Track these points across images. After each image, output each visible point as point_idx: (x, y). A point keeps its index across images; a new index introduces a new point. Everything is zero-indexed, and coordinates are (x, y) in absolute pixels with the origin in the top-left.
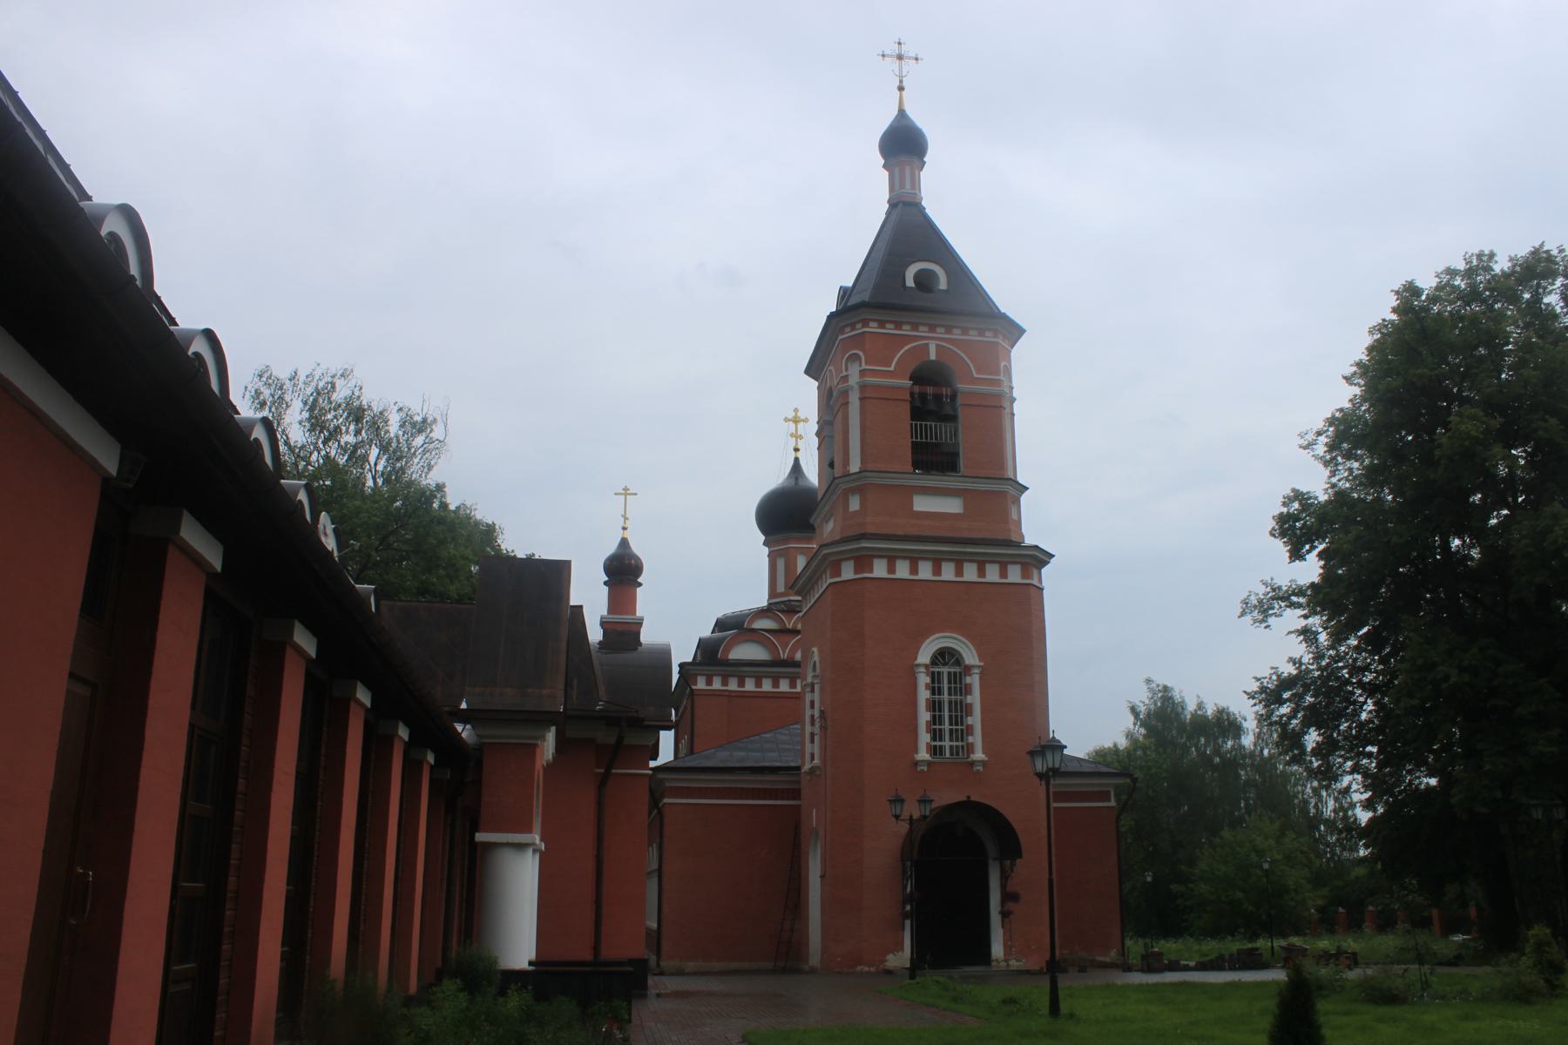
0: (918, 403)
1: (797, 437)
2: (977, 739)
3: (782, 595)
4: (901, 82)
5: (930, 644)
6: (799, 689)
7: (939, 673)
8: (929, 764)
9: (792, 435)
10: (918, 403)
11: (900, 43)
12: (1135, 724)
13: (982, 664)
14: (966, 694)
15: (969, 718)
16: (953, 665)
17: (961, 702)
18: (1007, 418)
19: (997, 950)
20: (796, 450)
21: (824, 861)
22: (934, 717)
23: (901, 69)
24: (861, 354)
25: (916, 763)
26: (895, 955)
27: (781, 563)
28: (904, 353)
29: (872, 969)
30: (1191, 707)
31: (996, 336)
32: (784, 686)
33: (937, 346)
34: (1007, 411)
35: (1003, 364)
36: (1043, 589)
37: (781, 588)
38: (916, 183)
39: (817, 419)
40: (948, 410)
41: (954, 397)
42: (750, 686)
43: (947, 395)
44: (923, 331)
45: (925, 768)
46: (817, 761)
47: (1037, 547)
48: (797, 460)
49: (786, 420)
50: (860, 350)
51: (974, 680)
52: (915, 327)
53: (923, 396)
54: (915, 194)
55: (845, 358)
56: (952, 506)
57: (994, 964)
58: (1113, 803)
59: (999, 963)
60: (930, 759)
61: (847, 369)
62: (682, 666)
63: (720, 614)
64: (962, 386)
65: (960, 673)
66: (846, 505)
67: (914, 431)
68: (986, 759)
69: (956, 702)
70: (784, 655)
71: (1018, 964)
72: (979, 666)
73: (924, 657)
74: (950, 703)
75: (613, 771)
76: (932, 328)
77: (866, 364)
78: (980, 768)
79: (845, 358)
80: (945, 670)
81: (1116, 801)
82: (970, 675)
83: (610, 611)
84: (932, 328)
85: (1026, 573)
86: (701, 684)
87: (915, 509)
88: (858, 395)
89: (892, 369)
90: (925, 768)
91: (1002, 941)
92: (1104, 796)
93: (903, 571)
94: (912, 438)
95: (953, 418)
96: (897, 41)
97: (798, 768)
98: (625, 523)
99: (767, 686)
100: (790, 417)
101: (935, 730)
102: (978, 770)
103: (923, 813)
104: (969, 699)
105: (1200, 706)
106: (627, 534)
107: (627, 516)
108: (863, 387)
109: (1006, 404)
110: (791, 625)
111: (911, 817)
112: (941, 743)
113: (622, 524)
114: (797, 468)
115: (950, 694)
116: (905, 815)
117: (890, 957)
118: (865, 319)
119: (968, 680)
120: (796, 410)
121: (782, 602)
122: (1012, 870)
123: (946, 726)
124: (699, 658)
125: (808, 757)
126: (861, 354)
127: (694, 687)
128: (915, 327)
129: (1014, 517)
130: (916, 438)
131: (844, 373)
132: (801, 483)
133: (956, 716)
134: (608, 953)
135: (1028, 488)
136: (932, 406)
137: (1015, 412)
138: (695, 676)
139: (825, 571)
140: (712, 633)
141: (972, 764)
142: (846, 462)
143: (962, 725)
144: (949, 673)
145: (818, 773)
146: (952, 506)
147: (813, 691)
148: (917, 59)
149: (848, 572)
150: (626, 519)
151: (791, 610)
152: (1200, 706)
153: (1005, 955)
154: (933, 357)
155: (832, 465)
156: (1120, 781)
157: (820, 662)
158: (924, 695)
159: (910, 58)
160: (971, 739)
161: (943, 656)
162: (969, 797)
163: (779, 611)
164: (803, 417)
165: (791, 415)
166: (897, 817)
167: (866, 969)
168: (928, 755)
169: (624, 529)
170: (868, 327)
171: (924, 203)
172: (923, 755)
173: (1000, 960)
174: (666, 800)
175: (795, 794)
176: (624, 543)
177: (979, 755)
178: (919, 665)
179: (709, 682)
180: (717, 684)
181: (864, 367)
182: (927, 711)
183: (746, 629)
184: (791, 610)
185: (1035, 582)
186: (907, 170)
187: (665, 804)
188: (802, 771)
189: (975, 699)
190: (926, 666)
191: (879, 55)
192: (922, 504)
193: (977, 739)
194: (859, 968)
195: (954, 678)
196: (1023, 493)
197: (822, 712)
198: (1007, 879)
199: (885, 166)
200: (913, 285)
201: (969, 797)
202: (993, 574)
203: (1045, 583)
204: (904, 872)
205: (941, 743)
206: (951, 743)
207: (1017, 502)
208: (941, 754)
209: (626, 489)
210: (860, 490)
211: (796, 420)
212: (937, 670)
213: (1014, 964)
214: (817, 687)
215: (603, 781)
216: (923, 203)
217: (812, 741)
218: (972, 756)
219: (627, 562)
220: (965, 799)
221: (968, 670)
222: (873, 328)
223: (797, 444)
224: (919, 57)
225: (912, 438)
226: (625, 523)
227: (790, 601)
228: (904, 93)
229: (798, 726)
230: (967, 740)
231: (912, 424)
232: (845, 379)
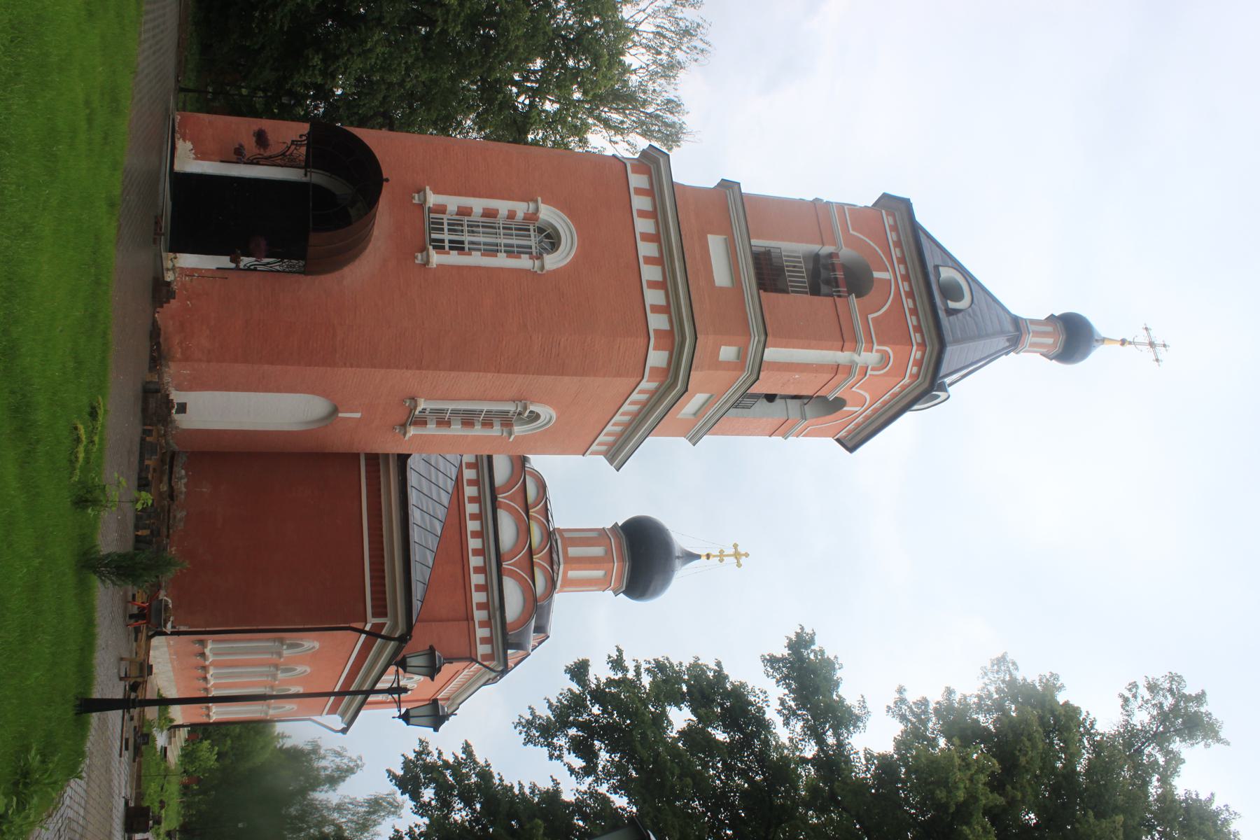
1: (721, 556)
2: (454, 258)
8: (422, 205)
9: (721, 552)
19: (188, 261)
25: (421, 190)
33: (890, 281)
37: (566, 535)
40: (824, 289)
43: (839, 291)
44: (900, 269)
45: (416, 201)
48: (698, 557)
49: (735, 546)
51: (524, 262)
53: (833, 268)
56: (721, 276)
57: (171, 255)
59: (171, 260)
70: (501, 498)
72: (542, 267)
73: (547, 213)
76: (906, 278)
89: (851, 232)
90: (416, 201)
91: (200, 266)
112: (446, 230)
117: (189, 145)
120: (747, 555)
128: (902, 260)
132: (677, 562)
136: (824, 274)
141: (423, 249)
146: (721, 276)
153: (182, 269)
154: (876, 275)
161: (551, 239)
162: (387, 180)
165: (741, 550)
172: (433, 199)
177: (436, 258)
192: (716, 244)
201: (387, 180)
205: (446, 230)
211: (737, 555)
212: (532, 233)
220: (384, 177)
228: (1118, 345)
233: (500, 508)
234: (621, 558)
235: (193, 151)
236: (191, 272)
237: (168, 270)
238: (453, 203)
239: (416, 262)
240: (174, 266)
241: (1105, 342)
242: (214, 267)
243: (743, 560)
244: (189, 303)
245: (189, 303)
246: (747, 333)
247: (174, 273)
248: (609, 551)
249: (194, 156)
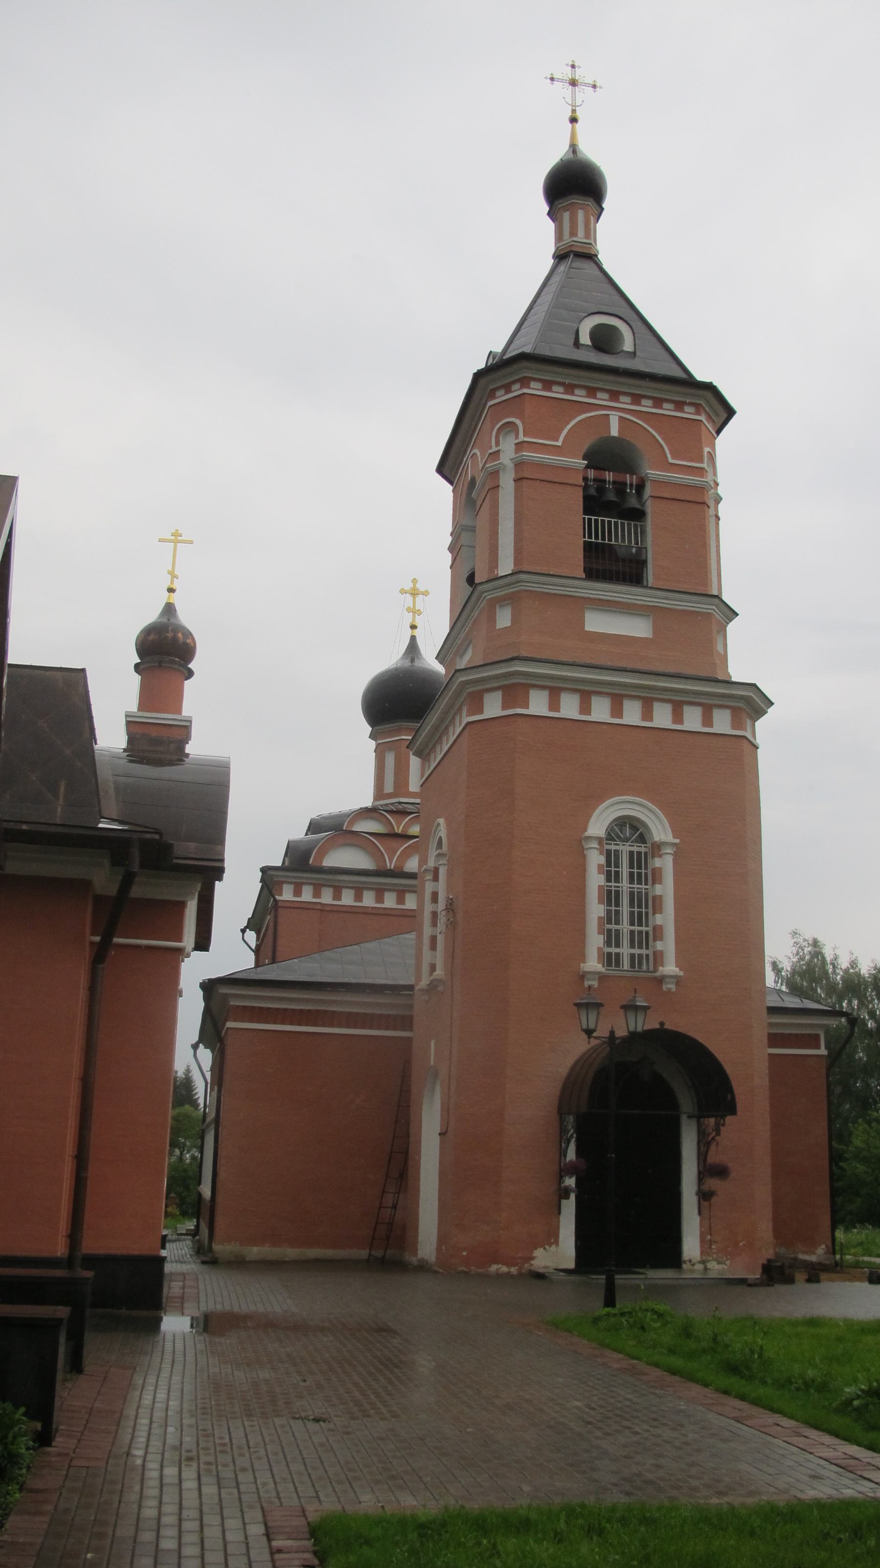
0: (592, 492)
1: (415, 612)
2: (668, 946)
3: (390, 796)
4: (574, 111)
5: (607, 808)
6: (411, 903)
7: (616, 851)
8: (602, 978)
9: (409, 610)
10: (592, 492)
11: (573, 66)
12: (776, 982)
13: (677, 841)
14: (654, 883)
15: (658, 916)
16: (636, 841)
17: (646, 894)
18: (712, 520)
20: (413, 627)
21: (446, 1110)
22: (609, 912)
23: (574, 98)
24: (518, 422)
25: (583, 976)
26: (544, 1249)
27: (390, 759)
28: (573, 426)
29: (514, 1270)
30: (844, 963)
31: (698, 413)
32: (390, 901)
33: (620, 418)
34: (711, 511)
35: (707, 450)
36: (757, 748)
37: (389, 788)
38: (590, 232)
39: (450, 530)
40: (633, 503)
41: (640, 487)
42: (347, 899)
43: (631, 485)
44: (602, 399)
46: (439, 973)
47: (754, 685)
48: (413, 638)
49: (403, 592)
50: (517, 418)
51: (666, 864)
52: (592, 392)
53: (600, 482)
54: (590, 244)
55: (496, 429)
57: (685, 1266)
58: (823, 1051)
59: (693, 1265)
60: (603, 970)
61: (497, 444)
62: (264, 870)
63: (314, 816)
64: (652, 473)
65: (646, 853)
66: (492, 619)
67: (588, 528)
68: (682, 973)
69: (639, 893)
70: (391, 864)
71: (720, 1267)
72: (674, 844)
74: (632, 894)
75: (116, 940)
76: (615, 395)
77: (525, 436)
78: (673, 987)
79: (496, 429)
80: (625, 849)
81: (826, 1048)
82: (660, 856)
83: (142, 706)
84: (615, 395)
85: (737, 723)
86: (287, 894)
87: (587, 628)
88: (513, 476)
89: (559, 443)
90: (595, 984)
91: (698, 1233)
92: (811, 1041)
93: (570, 707)
94: (584, 537)
95: (638, 515)
96: (571, 63)
97: (411, 988)
98: (172, 582)
99: (369, 900)
100: (407, 588)
101: (609, 931)
102: (669, 990)
103: (632, 1028)
104: (658, 889)
105: (854, 964)
106: (175, 599)
107: (176, 573)
108: (519, 465)
109: (711, 503)
110: (401, 828)
111: (612, 1033)
112: (617, 950)
113: (168, 584)
114: (413, 648)
115: (631, 881)
116: (602, 1032)
117: (539, 1253)
118: (525, 377)
119: (657, 863)
120: (414, 581)
121: (392, 804)
122: (718, 1134)
123: (625, 927)
124: (287, 864)
125: (425, 968)
126: (518, 422)
127: (278, 898)
129: (720, 648)
130: (590, 537)
131: (494, 449)
132: (417, 664)
133: (640, 914)
134: (91, 1245)
135: (737, 615)
136: (611, 496)
137: (720, 515)
138: (281, 884)
139: (460, 709)
140: (306, 834)
141: (661, 980)
142: (494, 562)
143: (647, 926)
144: (631, 853)
145: (440, 988)
147: (436, 878)
148: (594, 86)
149: (493, 707)
150: (174, 576)
151: (401, 812)
152: (854, 964)
153: (702, 1253)
154: (614, 432)
155: (471, 579)
156: (833, 1022)
157: (448, 837)
158: (595, 880)
159: (586, 85)
160: (659, 946)
162: (662, 1024)
163: (385, 811)
164: (422, 589)
165: (408, 586)
166: (589, 1032)
167: (504, 1269)
168: (600, 966)
169: (171, 590)
170: (529, 387)
171: (601, 257)
172: (593, 964)
173: (694, 1261)
174: (230, 1024)
175: (406, 1022)
176: (169, 609)
178: (589, 838)
179: (297, 892)
180: (307, 895)
181: (522, 438)
182: (600, 902)
183: (343, 830)
184: (401, 812)
185: (748, 735)
186: (581, 214)
187: (228, 1028)
188: (417, 988)
189: (666, 889)
190: (600, 840)
191: (546, 78)
193: (668, 946)
194: (494, 1268)
195: (637, 860)
196: (731, 621)
197: (450, 907)
198: (708, 1144)
199: (550, 214)
200: (589, 343)
201: (662, 1024)
202: (692, 720)
203: (759, 741)
204: (563, 1130)
205: (617, 950)
206: (633, 951)
207: (723, 630)
208: (618, 964)
209: (176, 534)
210: (512, 599)
211: (414, 593)
213: (716, 1268)
214: (442, 872)
215: (100, 954)
216: (599, 257)
217: (433, 946)
218: (660, 968)
219: (170, 635)
220: (658, 1026)
221: (657, 849)
222: (535, 389)
223: (414, 620)
224: (598, 84)
225: (584, 537)
226: (172, 582)
227: (400, 803)
228: (578, 126)
229: (413, 936)
230: (654, 946)
231: (584, 519)
232: (496, 455)
233: (403, 867)
235: (547, 1247)
236: (706, 1244)
237: (706, 1269)
238: (595, 941)
239: (674, 990)
240: (699, 1262)
241: (575, 143)
242: (697, 1219)
243: (421, 587)
244: (741, 1244)
245: (741, 1244)
246: (708, 616)
247: (709, 1261)
249: (554, 1246)
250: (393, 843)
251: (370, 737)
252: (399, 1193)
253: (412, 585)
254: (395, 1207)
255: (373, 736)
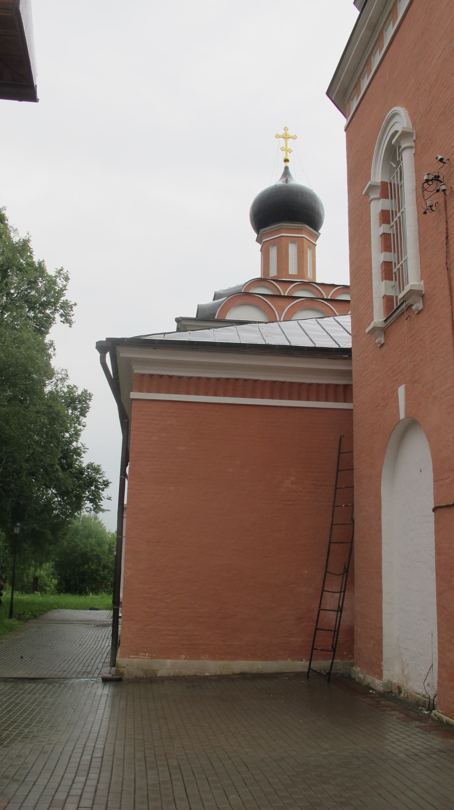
1: (286, 150)
9: (282, 149)
27: (273, 252)
48: (286, 168)
49: (277, 137)
120: (286, 129)
165: (282, 133)
211: (286, 137)
234: (299, 230)
243: (291, 133)
248: (293, 240)
250: (281, 302)
251: (256, 241)
252: (344, 592)
253: (284, 132)
254: (340, 610)
255: (259, 240)
